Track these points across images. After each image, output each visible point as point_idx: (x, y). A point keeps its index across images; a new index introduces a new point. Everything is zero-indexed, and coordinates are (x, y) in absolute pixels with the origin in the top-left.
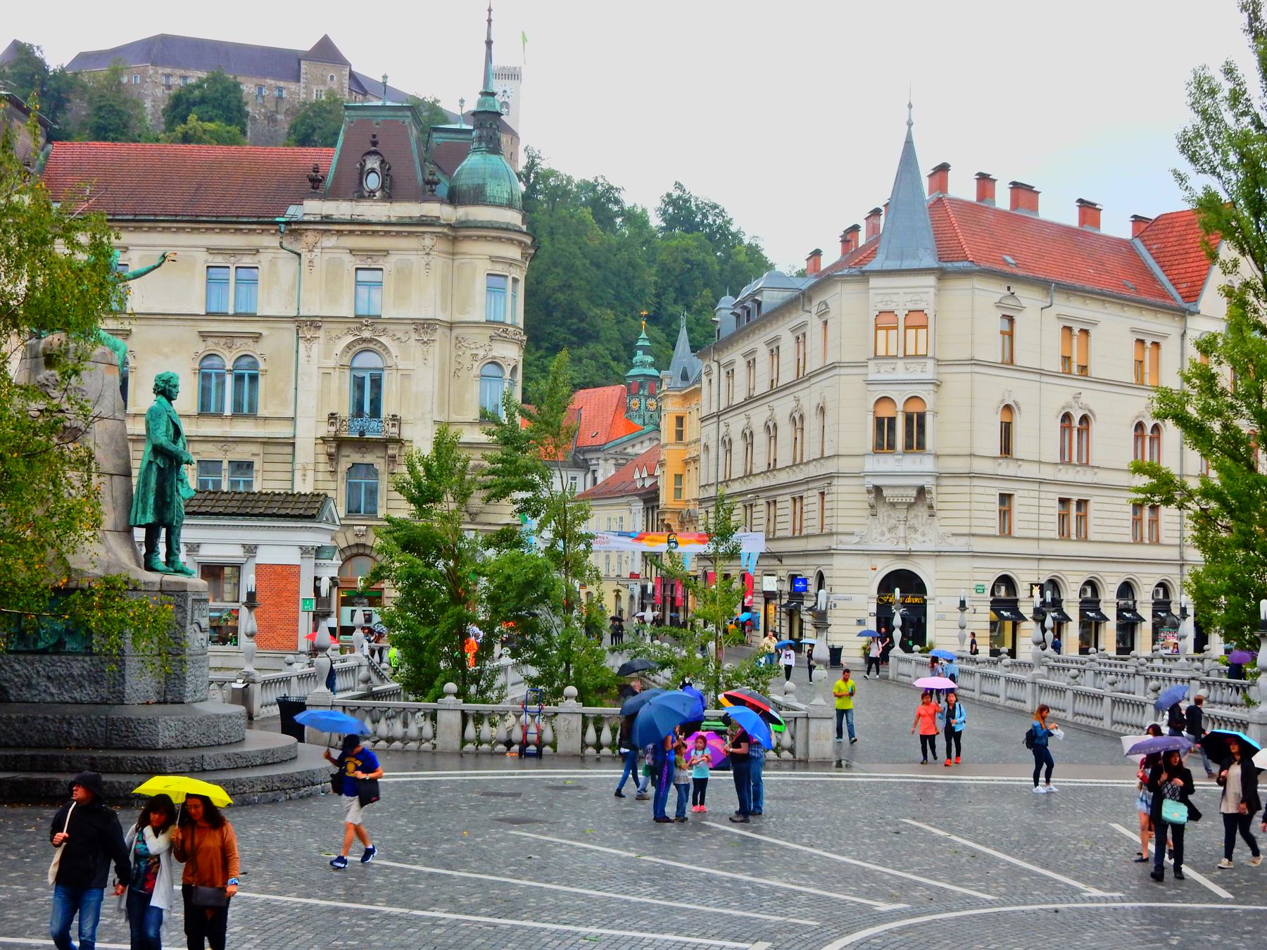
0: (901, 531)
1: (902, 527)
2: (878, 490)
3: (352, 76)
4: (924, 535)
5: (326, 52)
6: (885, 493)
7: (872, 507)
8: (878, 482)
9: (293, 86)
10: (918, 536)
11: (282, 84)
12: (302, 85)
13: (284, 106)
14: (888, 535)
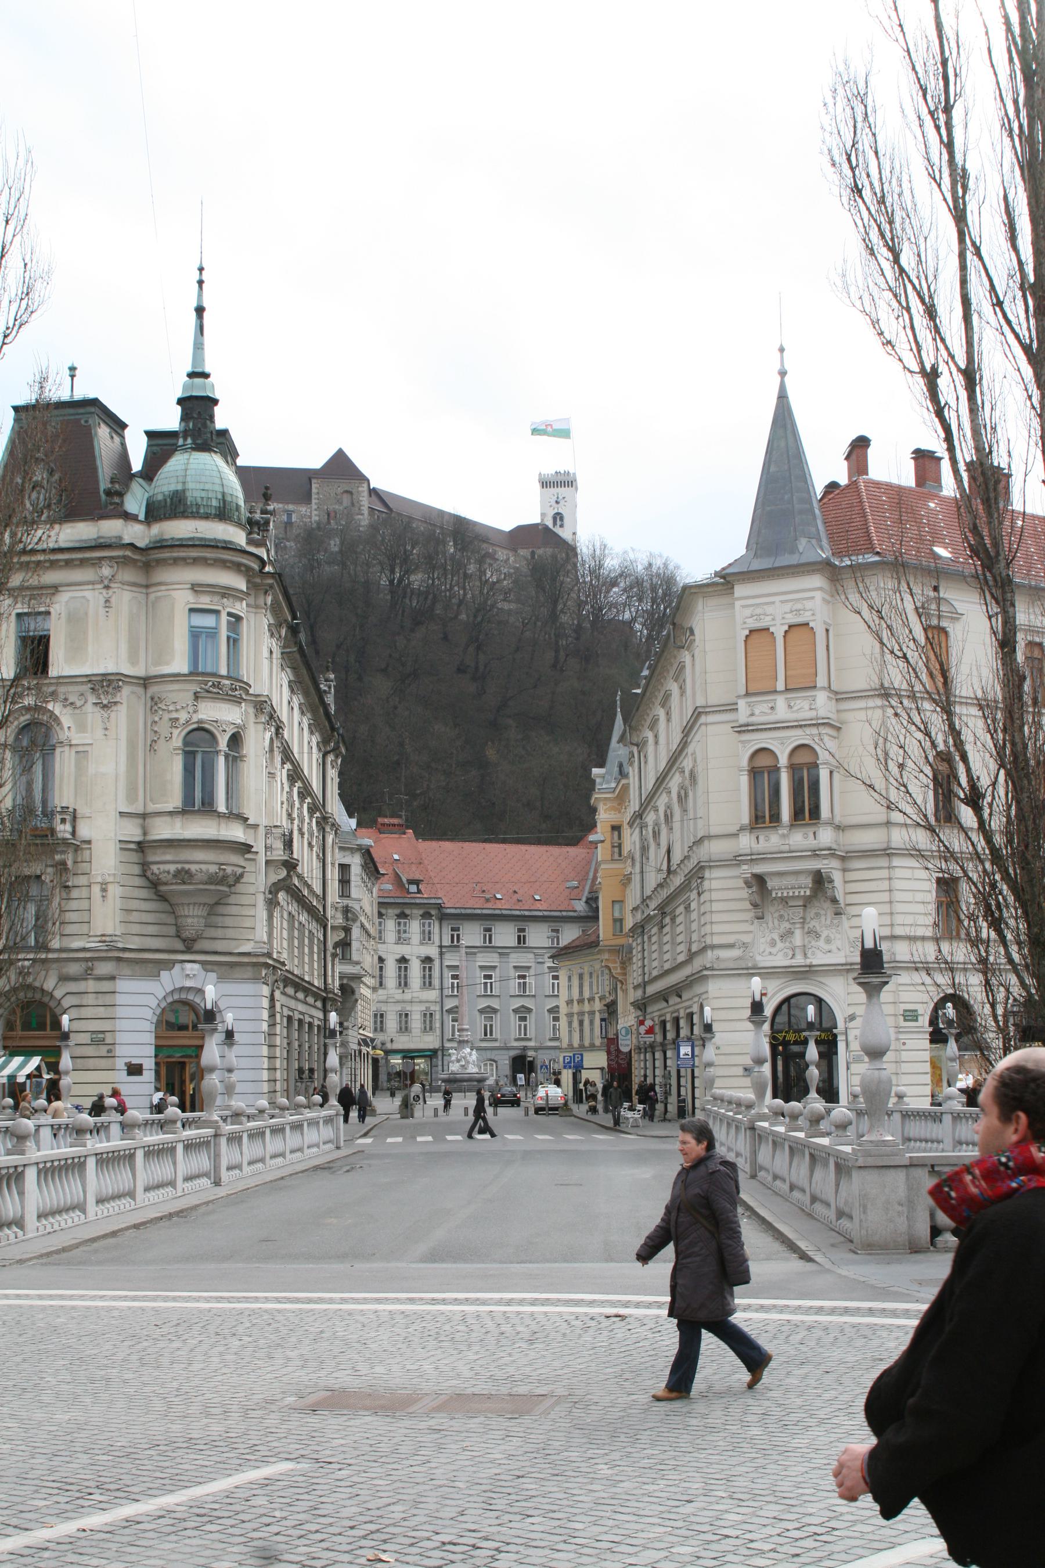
0: (798, 938)
1: (798, 933)
2: (760, 880)
3: (374, 492)
4: (828, 941)
5: (340, 466)
6: (770, 884)
7: (755, 905)
8: (759, 869)
9: (303, 509)
10: (821, 943)
11: (291, 507)
12: (314, 507)
13: (295, 531)
14: (780, 945)
